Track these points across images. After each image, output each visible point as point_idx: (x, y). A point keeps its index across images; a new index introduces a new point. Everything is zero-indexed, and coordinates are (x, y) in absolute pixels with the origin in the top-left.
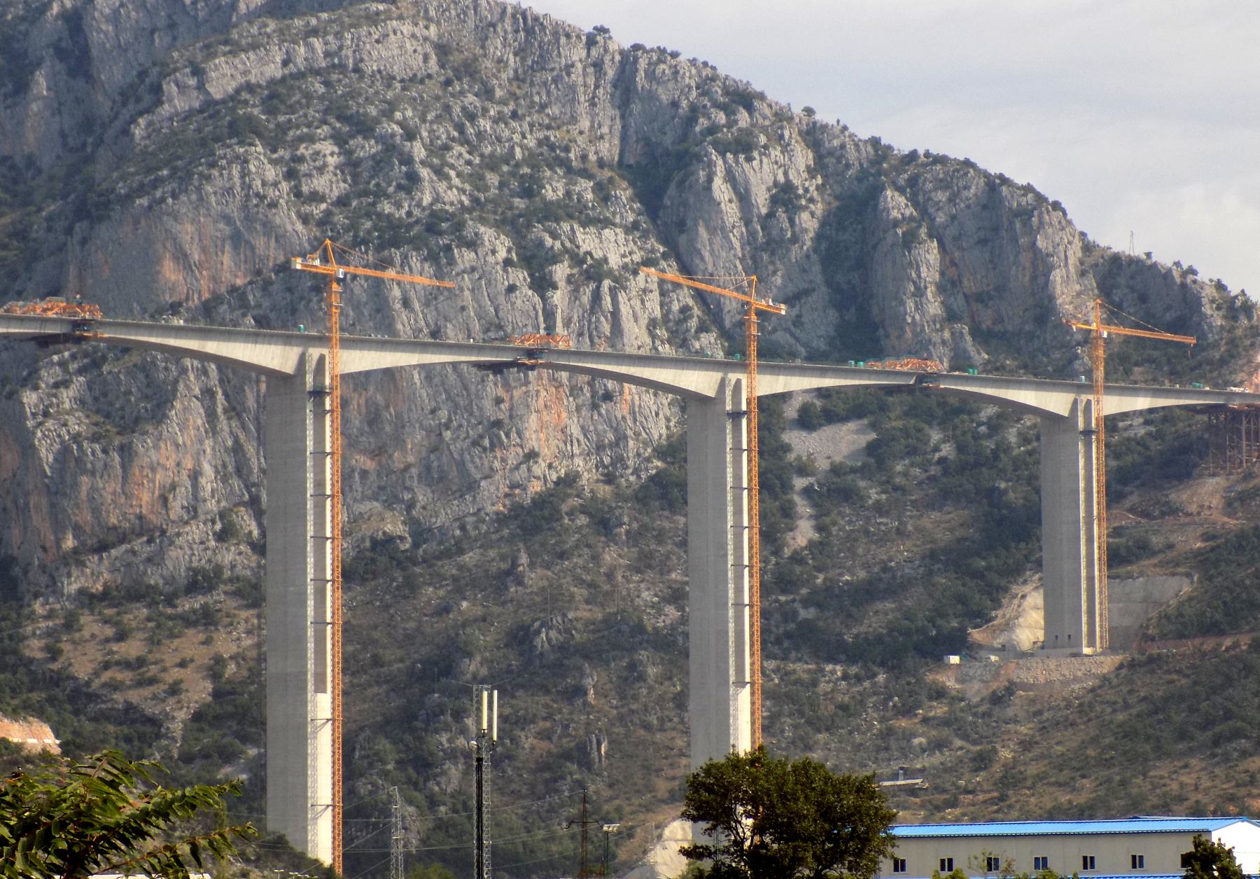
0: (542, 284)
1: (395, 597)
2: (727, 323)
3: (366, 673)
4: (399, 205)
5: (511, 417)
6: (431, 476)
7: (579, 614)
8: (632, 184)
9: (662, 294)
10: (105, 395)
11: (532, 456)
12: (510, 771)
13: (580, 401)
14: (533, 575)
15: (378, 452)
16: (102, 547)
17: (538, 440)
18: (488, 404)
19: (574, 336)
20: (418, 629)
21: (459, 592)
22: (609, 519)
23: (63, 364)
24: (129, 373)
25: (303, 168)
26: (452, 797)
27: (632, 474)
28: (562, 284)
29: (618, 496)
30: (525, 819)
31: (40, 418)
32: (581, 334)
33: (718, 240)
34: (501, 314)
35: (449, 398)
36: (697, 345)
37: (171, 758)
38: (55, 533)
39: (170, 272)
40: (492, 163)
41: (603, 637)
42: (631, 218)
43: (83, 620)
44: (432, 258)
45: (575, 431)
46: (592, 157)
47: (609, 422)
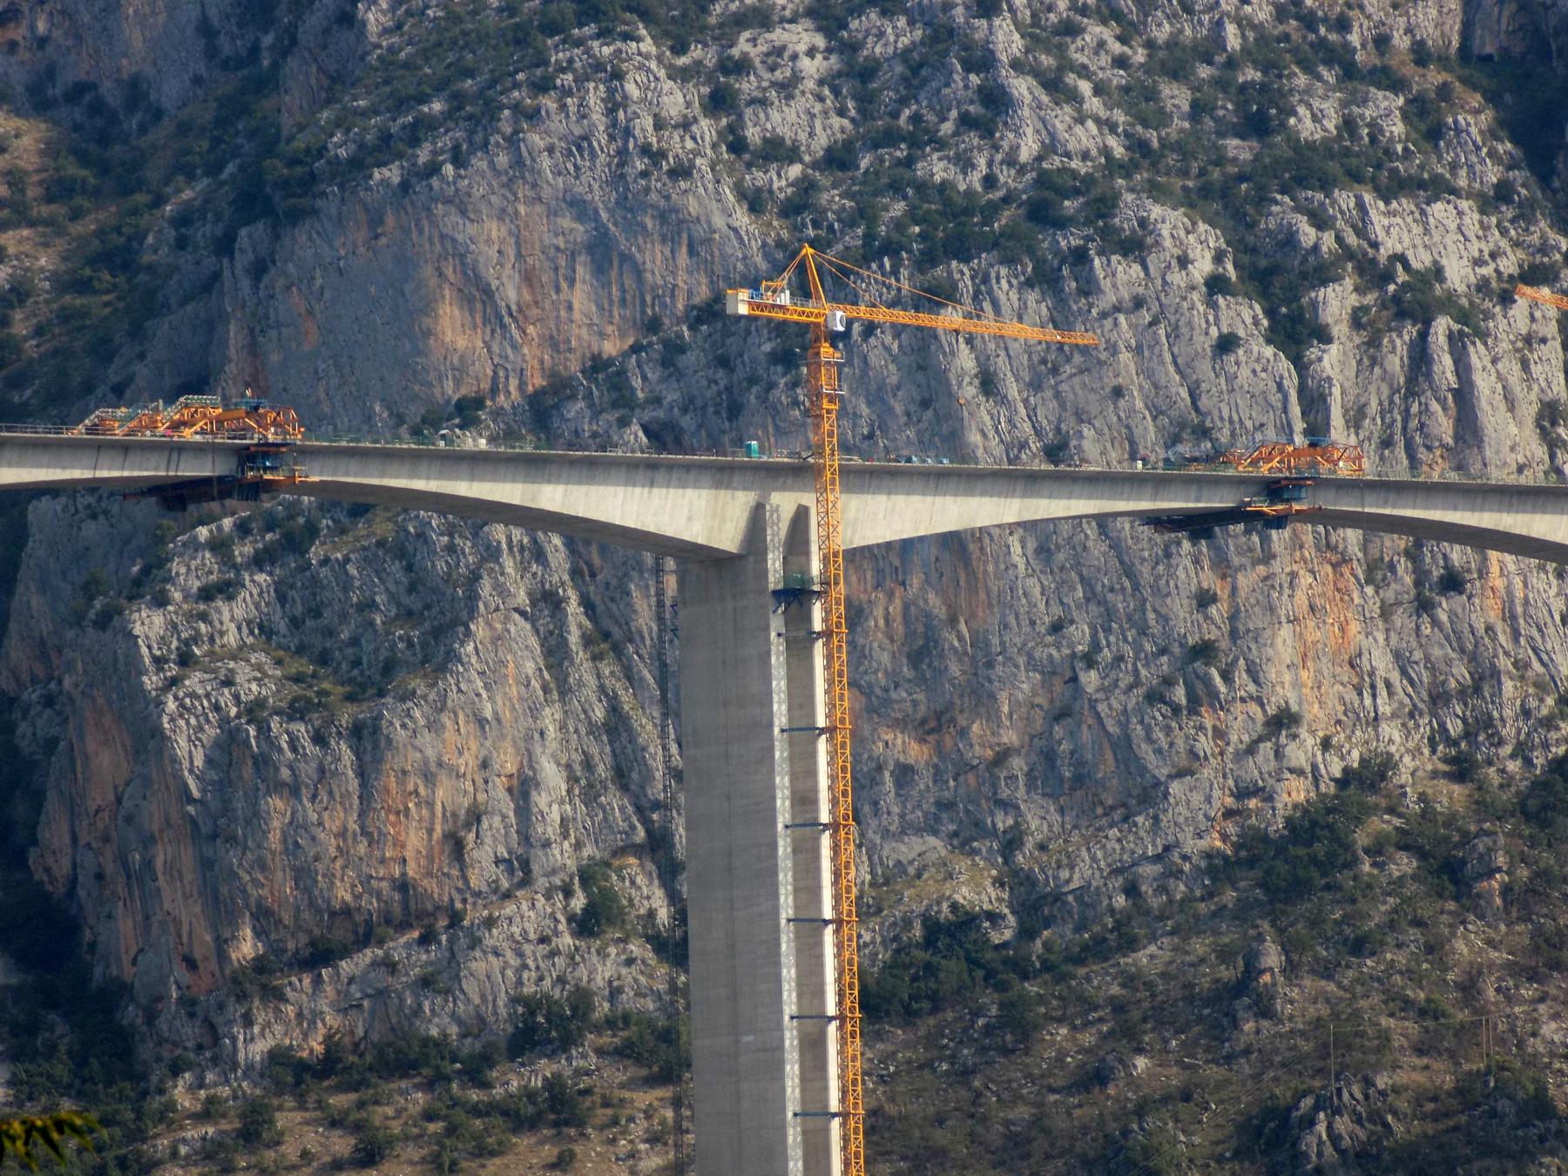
0: (1296, 332)
1: (983, 1050)
4: (966, 164)
5: (1234, 635)
7: (1402, 1077)
8: (1492, 98)
10: (317, 614)
11: (1283, 722)
13: (1389, 594)
14: (1295, 993)
15: (933, 725)
16: (319, 957)
17: (1297, 684)
18: (1180, 609)
19: (1371, 448)
20: (1036, 1121)
21: (1128, 1036)
22: (1463, 862)
23: (219, 546)
24: (369, 561)
25: (747, 86)
27: (1513, 756)
28: (1340, 330)
29: (1482, 806)
31: (173, 670)
32: (1387, 443)
34: (1204, 402)
35: (1091, 597)
38: (215, 928)
39: (453, 329)
40: (1174, 62)
41: (1456, 1128)
42: (1492, 174)
43: (282, 1120)
44: (1045, 279)
45: (1381, 662)
46: (1401, 42)
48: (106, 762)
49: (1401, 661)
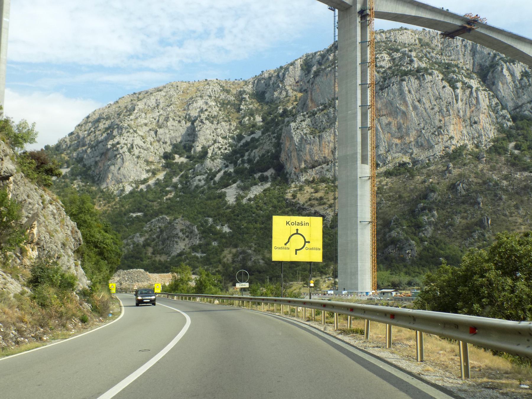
0: (454, 88)
2: (509, 110)
3: (396, 200)
4: (407, 67)
5: (445, 126)
6: (420, 146)
9: (489, 100)
11: (452, 138)
12: (452, 230)
13: (466, 124)
15: (401, 138)
16: (313, 167)
17: (454, 133)
21: (429, 176)
23: (304, 116)
24: (323, 116)
25: (378, 60)
26: (429, 238)
30: (460, 247)
32: (466, 104)
33: (505, 86)
34: (441, 95)
35: (424, 120)
36: (501, 113)
37: (327, 227)
38: (299, 163)
44: (418, 78)
45: (465, 132)
46: (464, 68)
47: (476, 130)
48: (288, 144)
49: (468, 133)
